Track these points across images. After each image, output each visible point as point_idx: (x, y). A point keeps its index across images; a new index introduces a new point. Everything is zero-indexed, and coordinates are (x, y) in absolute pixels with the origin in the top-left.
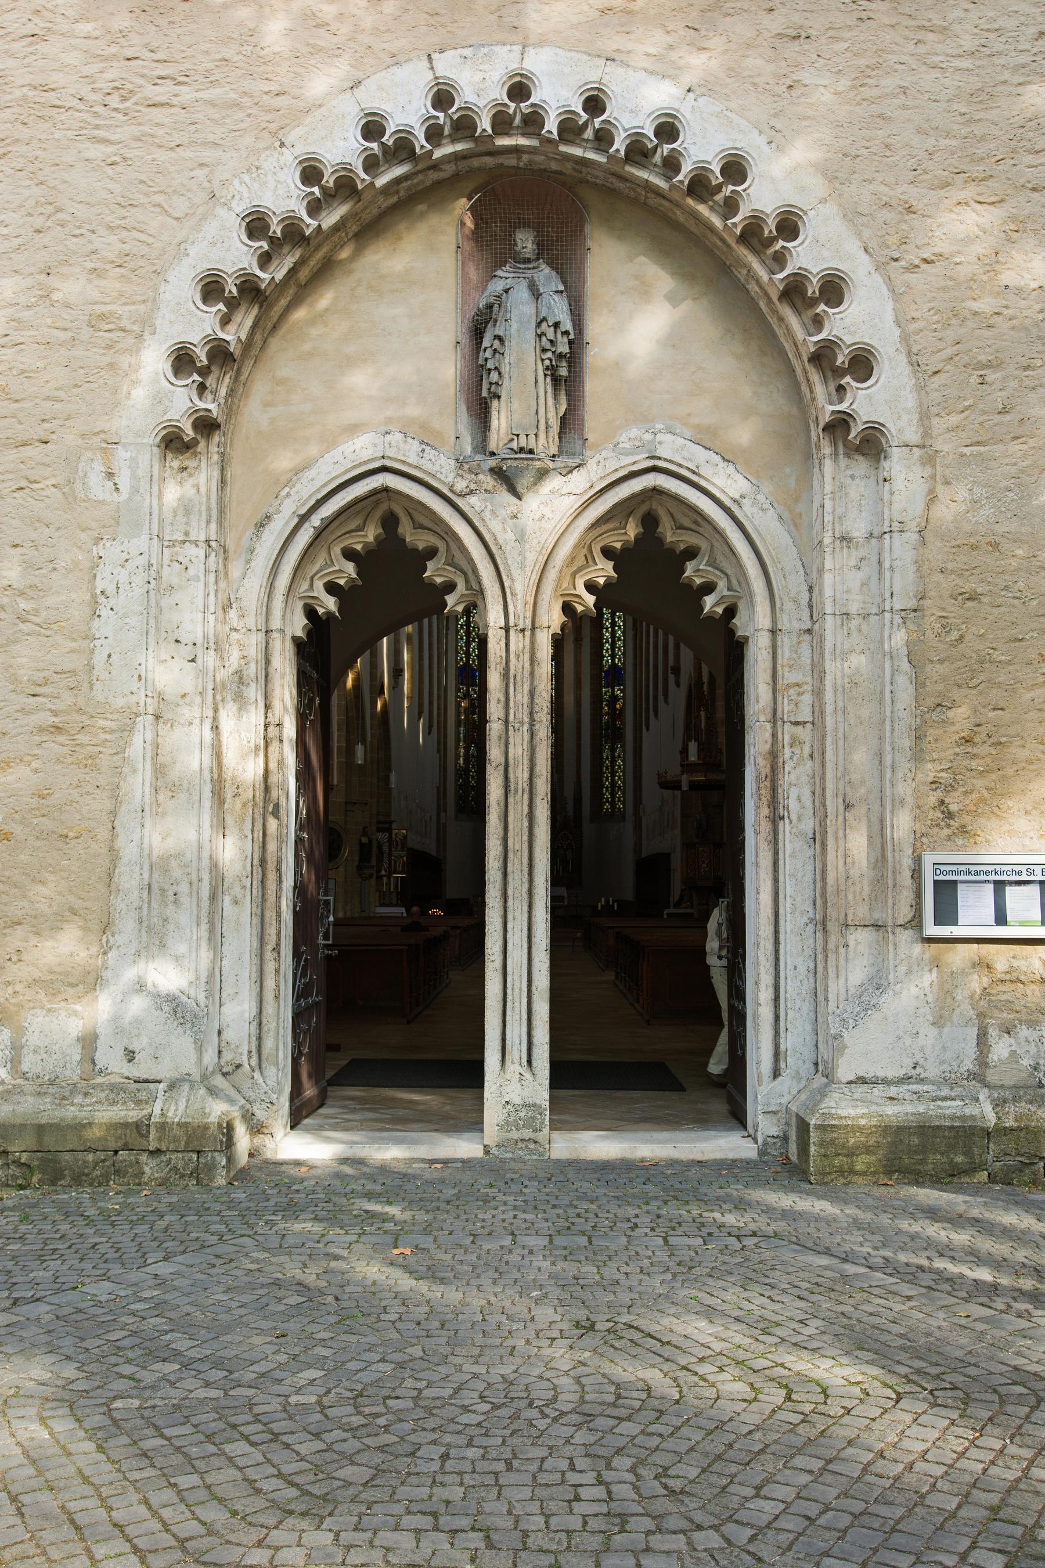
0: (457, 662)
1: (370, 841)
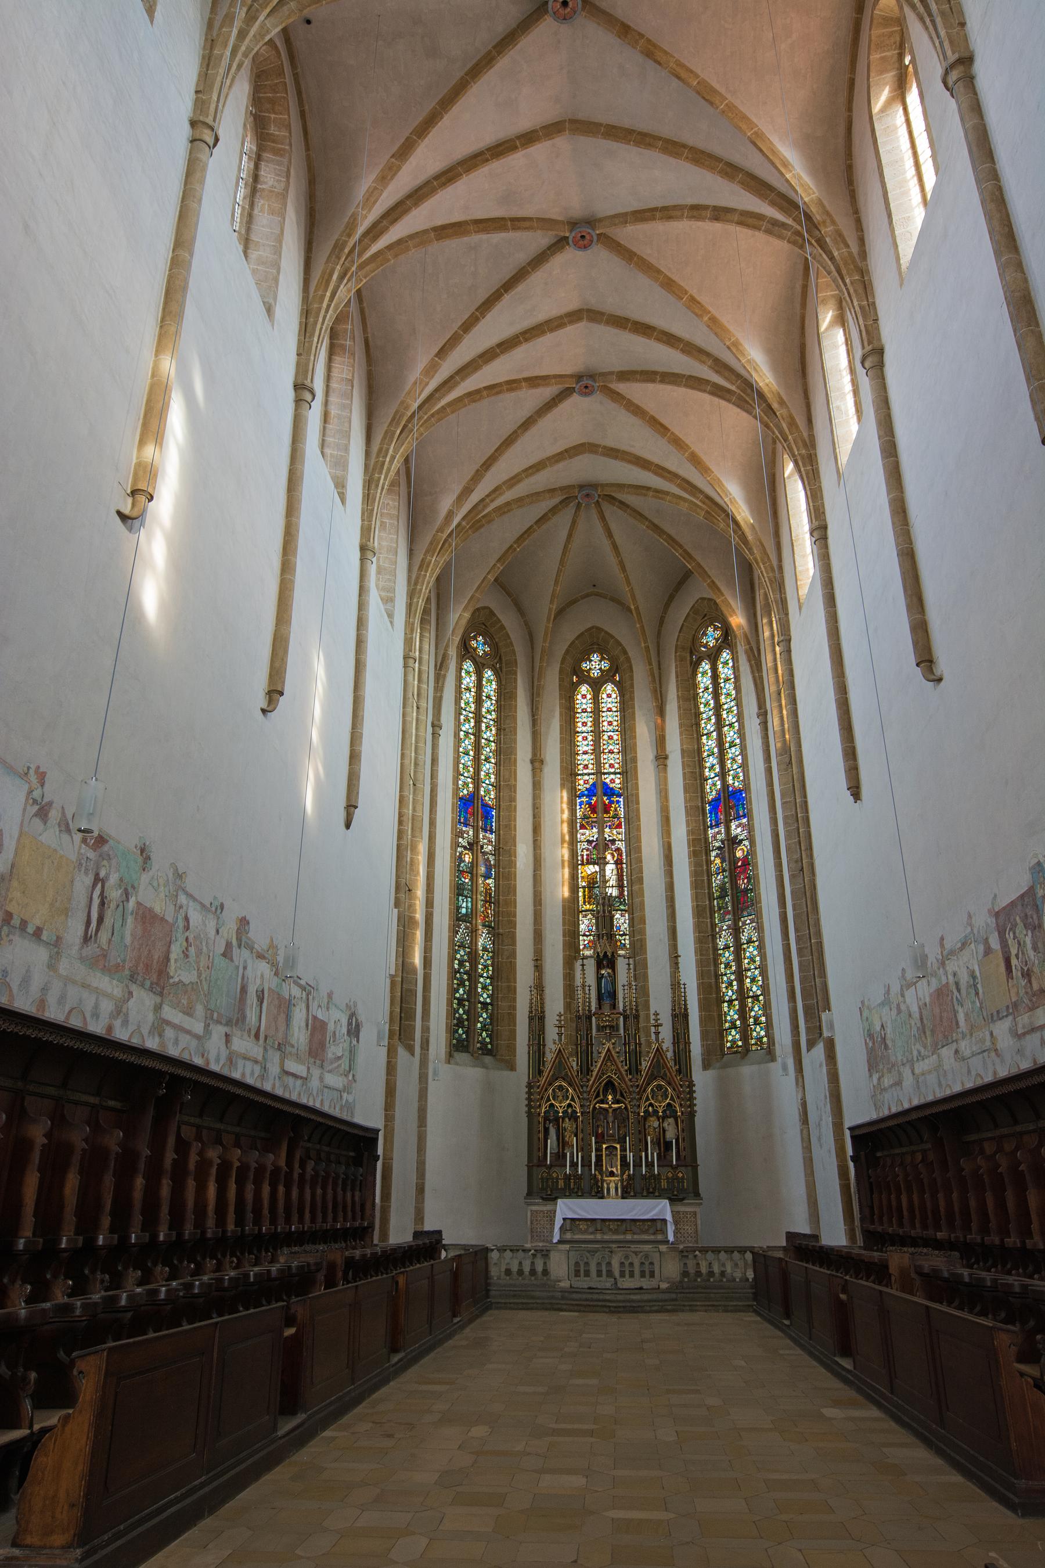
0: (456, 789)
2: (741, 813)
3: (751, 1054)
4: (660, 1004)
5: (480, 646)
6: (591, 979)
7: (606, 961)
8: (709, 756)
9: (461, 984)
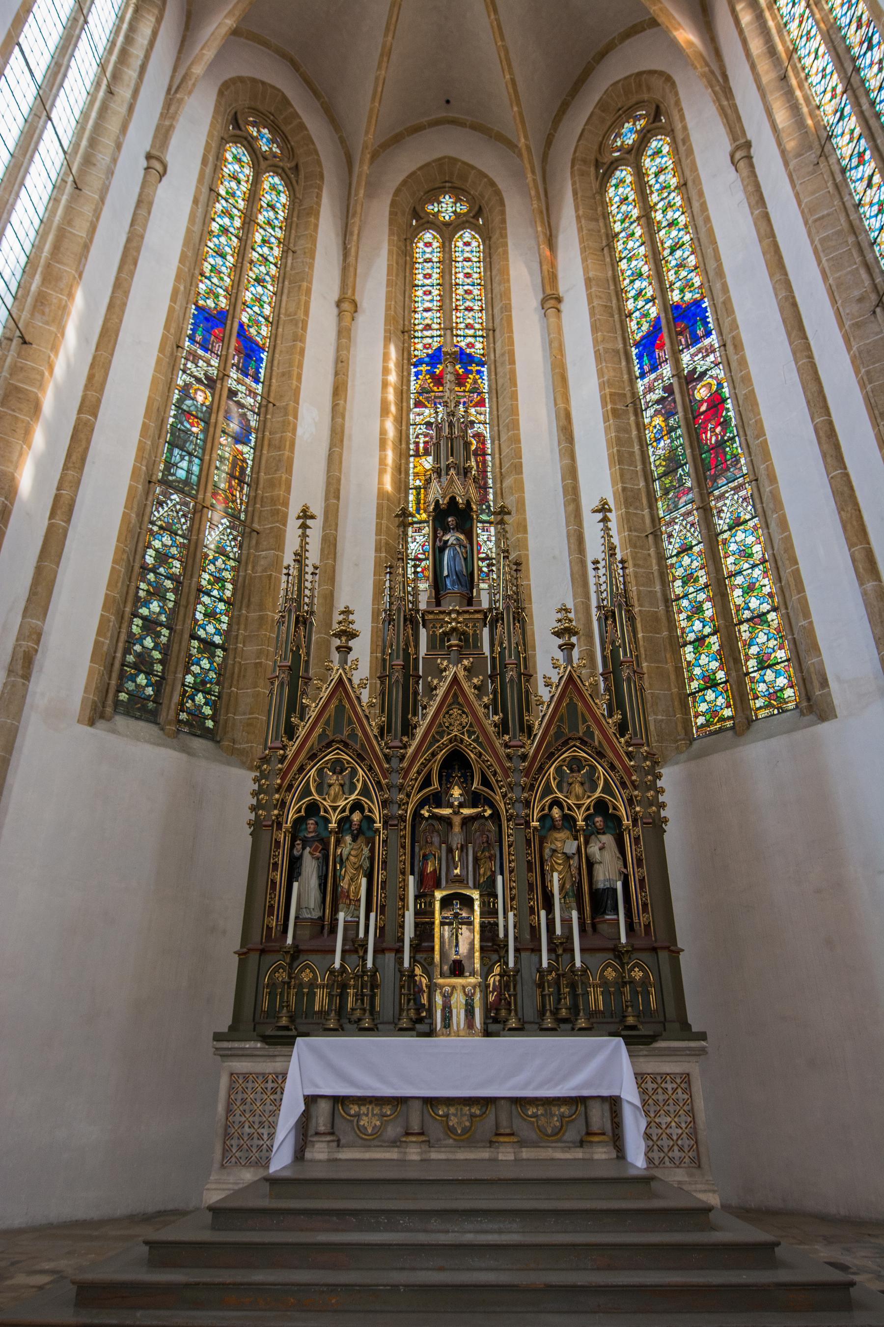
2: (700, 332)
3: (755, 726)
8: (632, 282)
9: (157, 593)
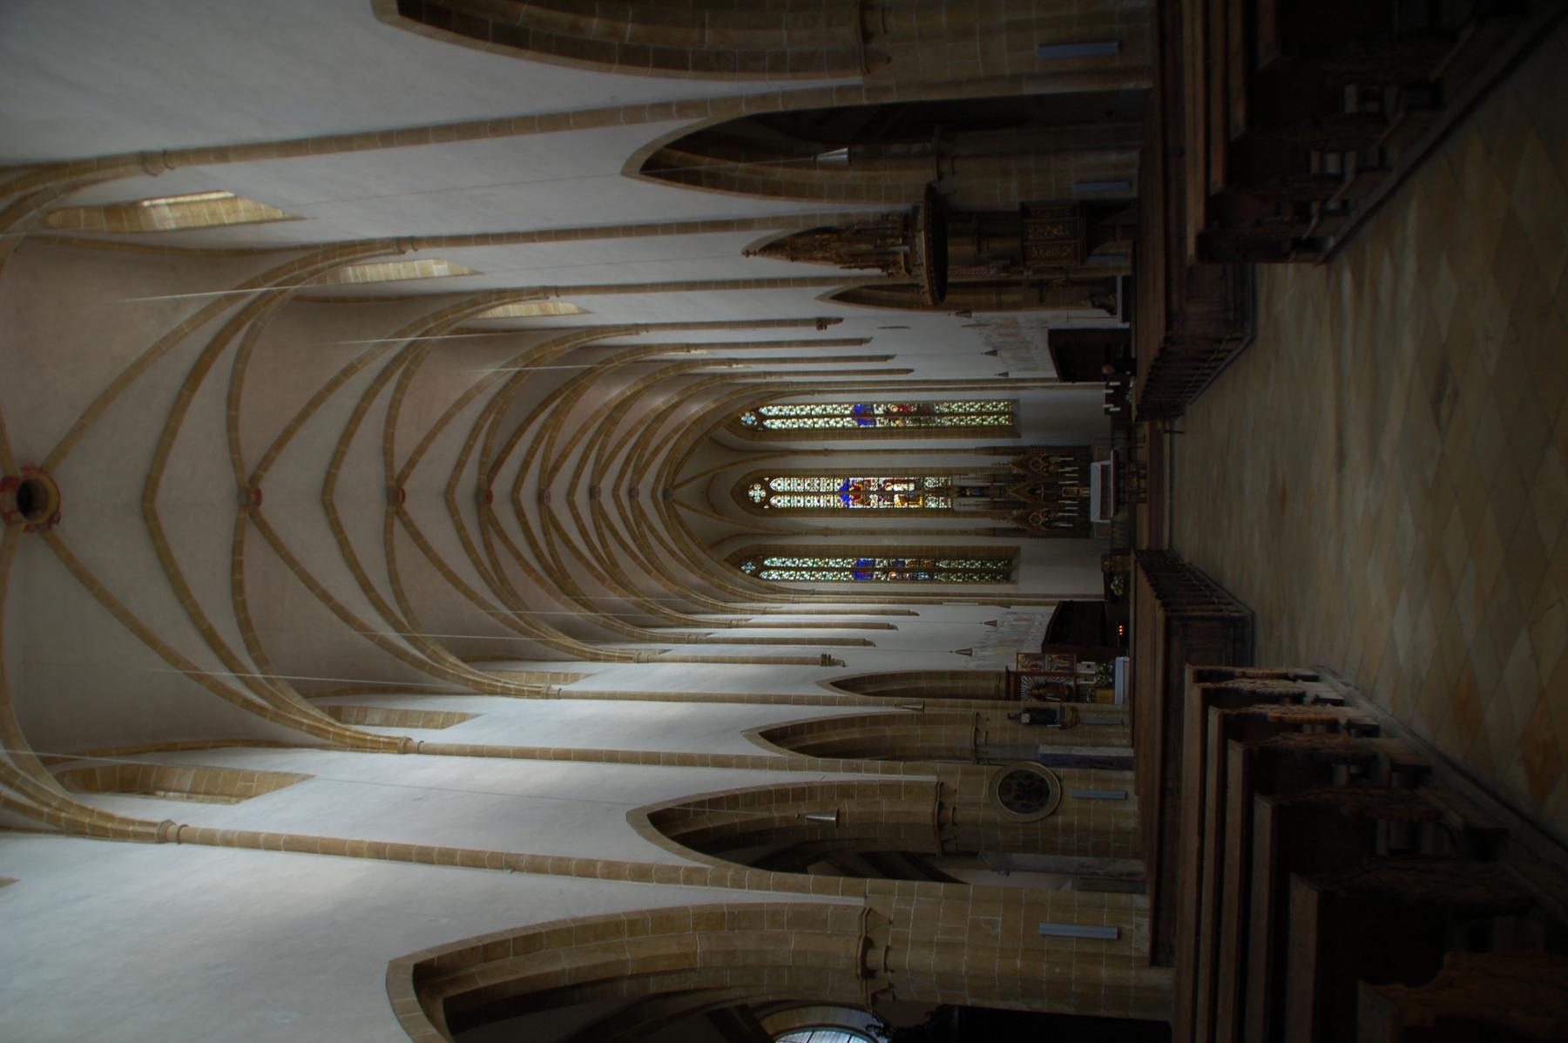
1: (1028, 710)
4: (987, 461)
5: (750, 567)
6: (972, 501)
7: (962, 492)
